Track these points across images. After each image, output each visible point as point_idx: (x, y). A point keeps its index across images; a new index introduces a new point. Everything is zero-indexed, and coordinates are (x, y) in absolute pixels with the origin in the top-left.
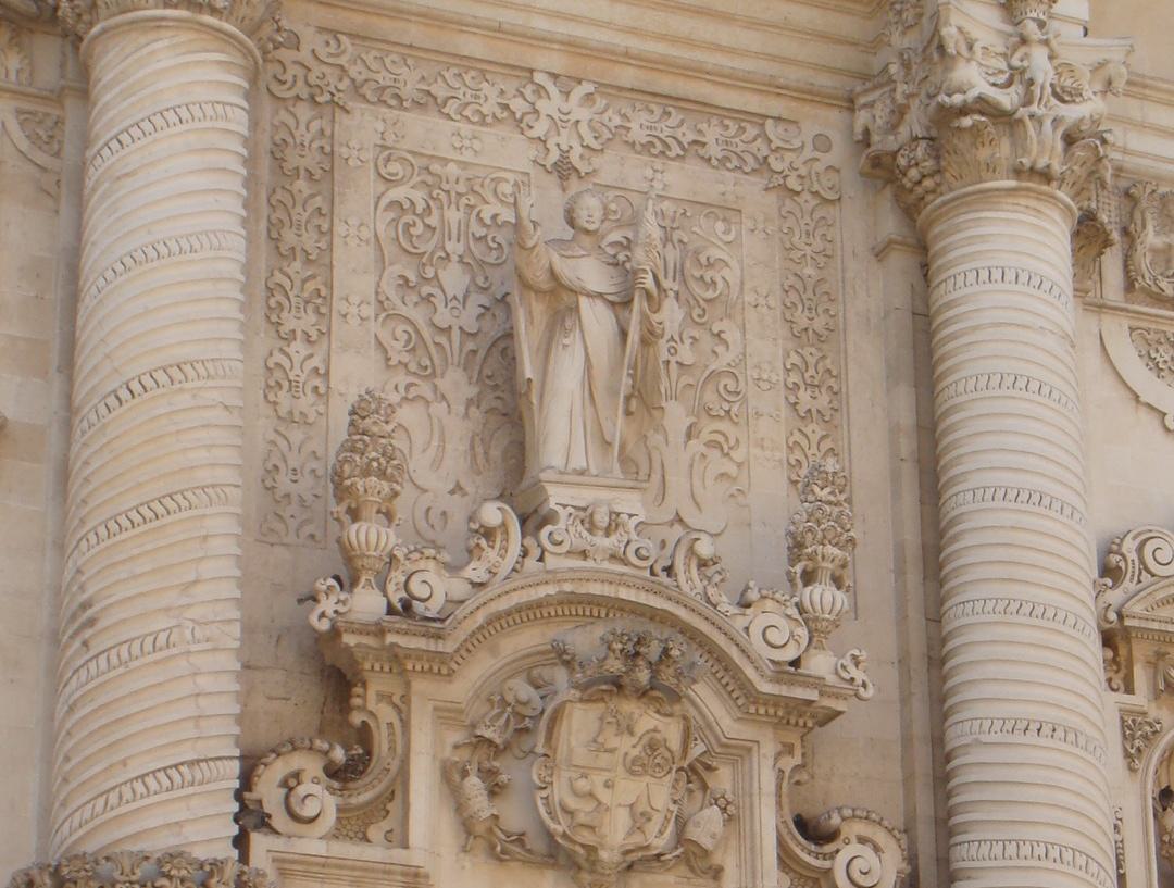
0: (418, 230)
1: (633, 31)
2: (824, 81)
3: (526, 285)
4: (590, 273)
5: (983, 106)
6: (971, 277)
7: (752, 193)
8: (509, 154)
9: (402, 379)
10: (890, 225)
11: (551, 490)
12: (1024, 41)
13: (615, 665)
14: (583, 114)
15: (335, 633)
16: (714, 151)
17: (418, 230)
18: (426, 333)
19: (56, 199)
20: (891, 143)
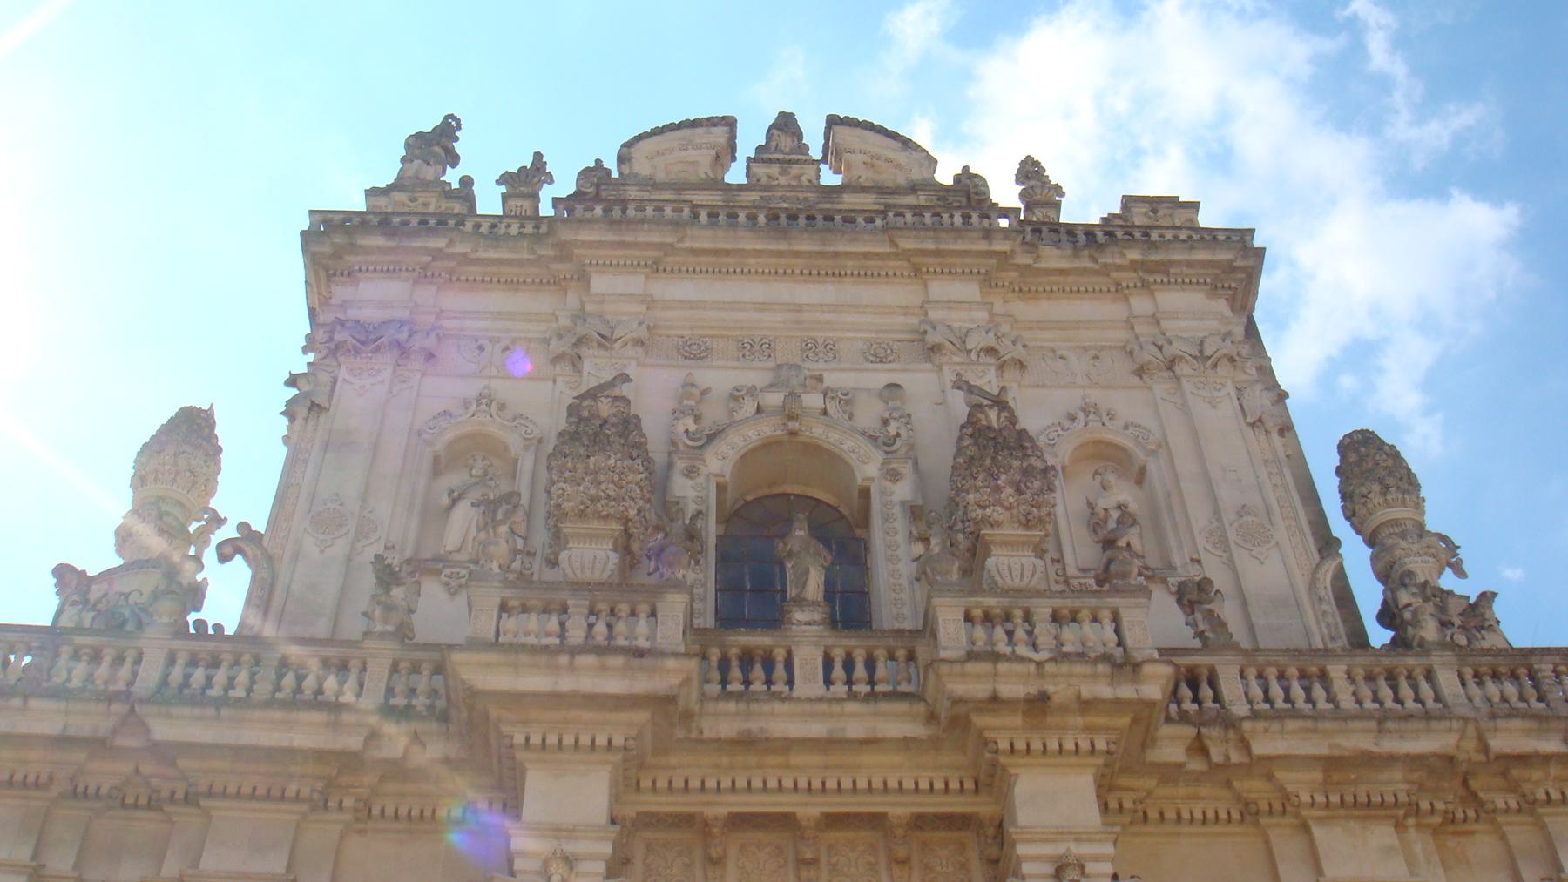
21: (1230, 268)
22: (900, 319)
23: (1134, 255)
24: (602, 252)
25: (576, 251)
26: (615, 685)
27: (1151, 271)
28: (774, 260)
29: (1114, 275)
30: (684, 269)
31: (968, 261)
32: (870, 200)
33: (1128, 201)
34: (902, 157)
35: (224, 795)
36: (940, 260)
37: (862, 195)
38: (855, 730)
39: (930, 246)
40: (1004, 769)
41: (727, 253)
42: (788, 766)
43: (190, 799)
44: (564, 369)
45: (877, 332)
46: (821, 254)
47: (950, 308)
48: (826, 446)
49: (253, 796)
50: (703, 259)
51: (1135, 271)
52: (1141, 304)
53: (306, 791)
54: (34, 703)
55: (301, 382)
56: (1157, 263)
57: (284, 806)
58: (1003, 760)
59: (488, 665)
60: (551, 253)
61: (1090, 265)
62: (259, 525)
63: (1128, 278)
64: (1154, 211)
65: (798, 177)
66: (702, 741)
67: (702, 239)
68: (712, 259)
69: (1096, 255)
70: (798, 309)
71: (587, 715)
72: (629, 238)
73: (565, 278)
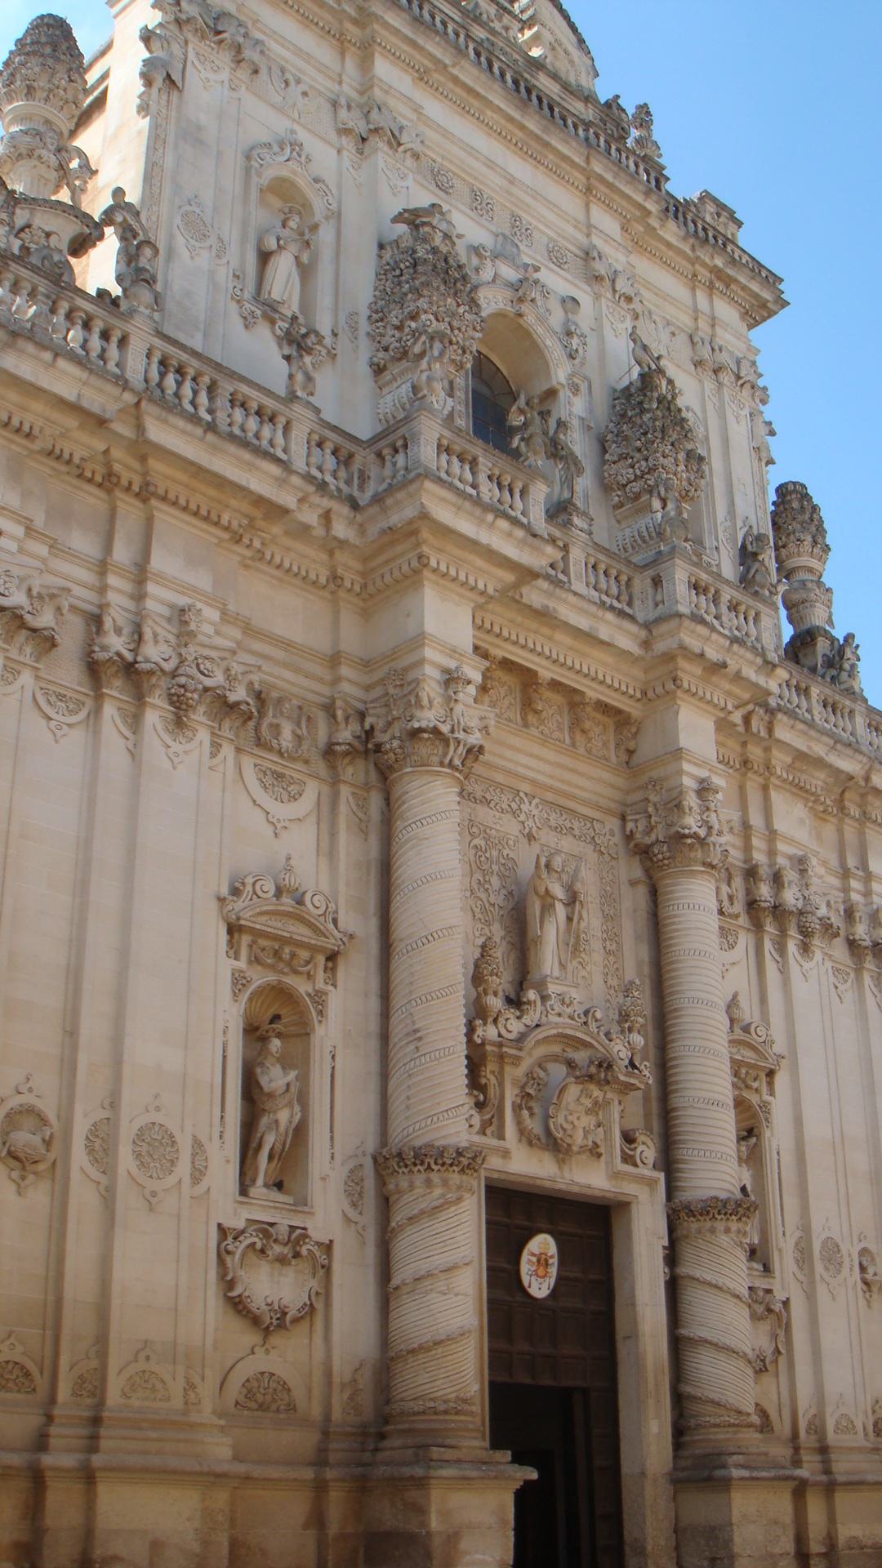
0: (483, 859)
1: (551, 777)
2: (613, 805)
3: (537, 893)
4: (558, 891)
5: (695, 836)
6: (686, 906)
7: (588, 850)
8: (510, 827)
9: (480, 926)
10: (638, 873)
11: (549, 985)
12: (708, 809)
13: (593, 1070)
14: (535, 812)
15: (483, 1044)
16: (577, 832)
17: (483, 859)
18: (487, 905)
19: (366, 834)
20: (648, 840)
21: (763, 305)
22: (571, 230)
23: (719, 262)
24: (393, 39)
25: (376, 27)
26: (511, 551)
27: (719, 279)
28: (503, 121)
29: (697, 267)
30: (441, 89)
31: (624, 203)
32: (556, 91)
33: (706, 197)
34: (575, 53)
35: (175, 504)
36: (607, 191)
37: (552, 82)
38: (604, 633)
39: (609, 177)
40: (674, 698)
41: (477, 95)
42: (550, 638)
43: (145, 494)
44: (348, 143)
45: (559, 235)
46: (537, 138)
47: (606, 241)
48: (535, 336)
49: (196, 514)
50: (458, 90)
51: (711, 272)
52: (702, 298)
53: (235, 524)
54: (62, 363)
55: (156, 44)
56: (729, 276)
57: (213, 530)
58: (679, 693)
59: (443, 499)
60: (353, 13)
61: (689, 252)
62: (132, 197)
63: (704, 274)
64: (719, 215)
65: (507, 29)
66: (518, 602)
67: (468, 73)
68: (464, 94)
69: (697, 247)
70: (512, 181)
71: (479, 562)
72: (421, 41)
73: (350, 41)
